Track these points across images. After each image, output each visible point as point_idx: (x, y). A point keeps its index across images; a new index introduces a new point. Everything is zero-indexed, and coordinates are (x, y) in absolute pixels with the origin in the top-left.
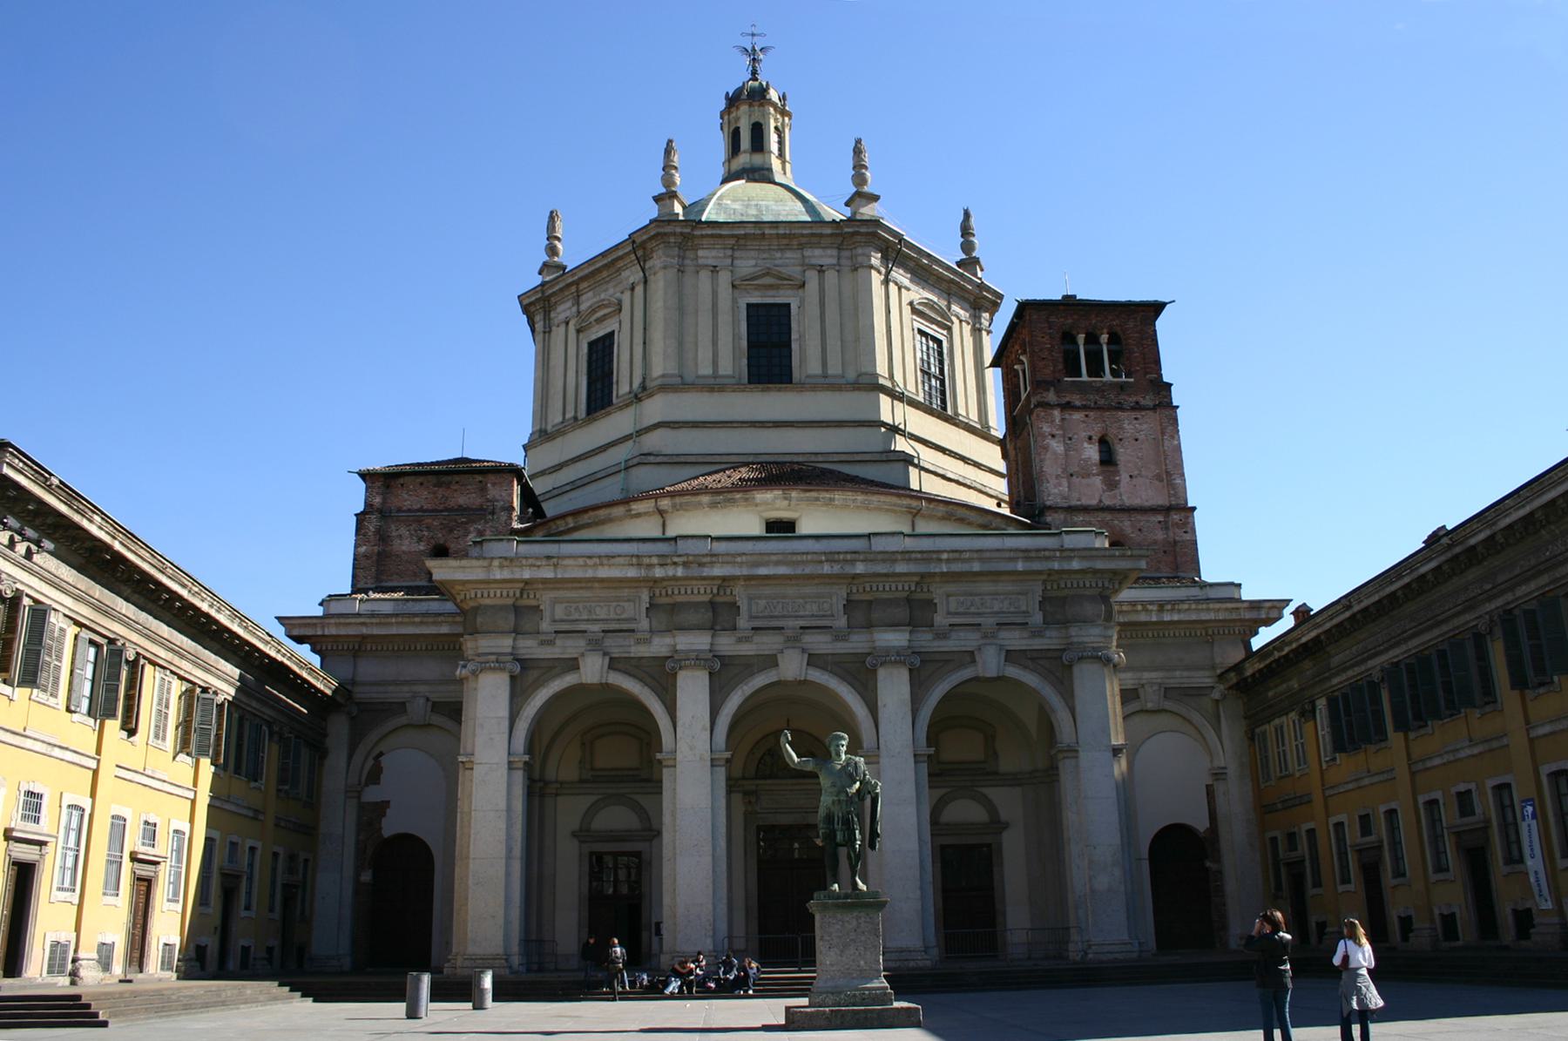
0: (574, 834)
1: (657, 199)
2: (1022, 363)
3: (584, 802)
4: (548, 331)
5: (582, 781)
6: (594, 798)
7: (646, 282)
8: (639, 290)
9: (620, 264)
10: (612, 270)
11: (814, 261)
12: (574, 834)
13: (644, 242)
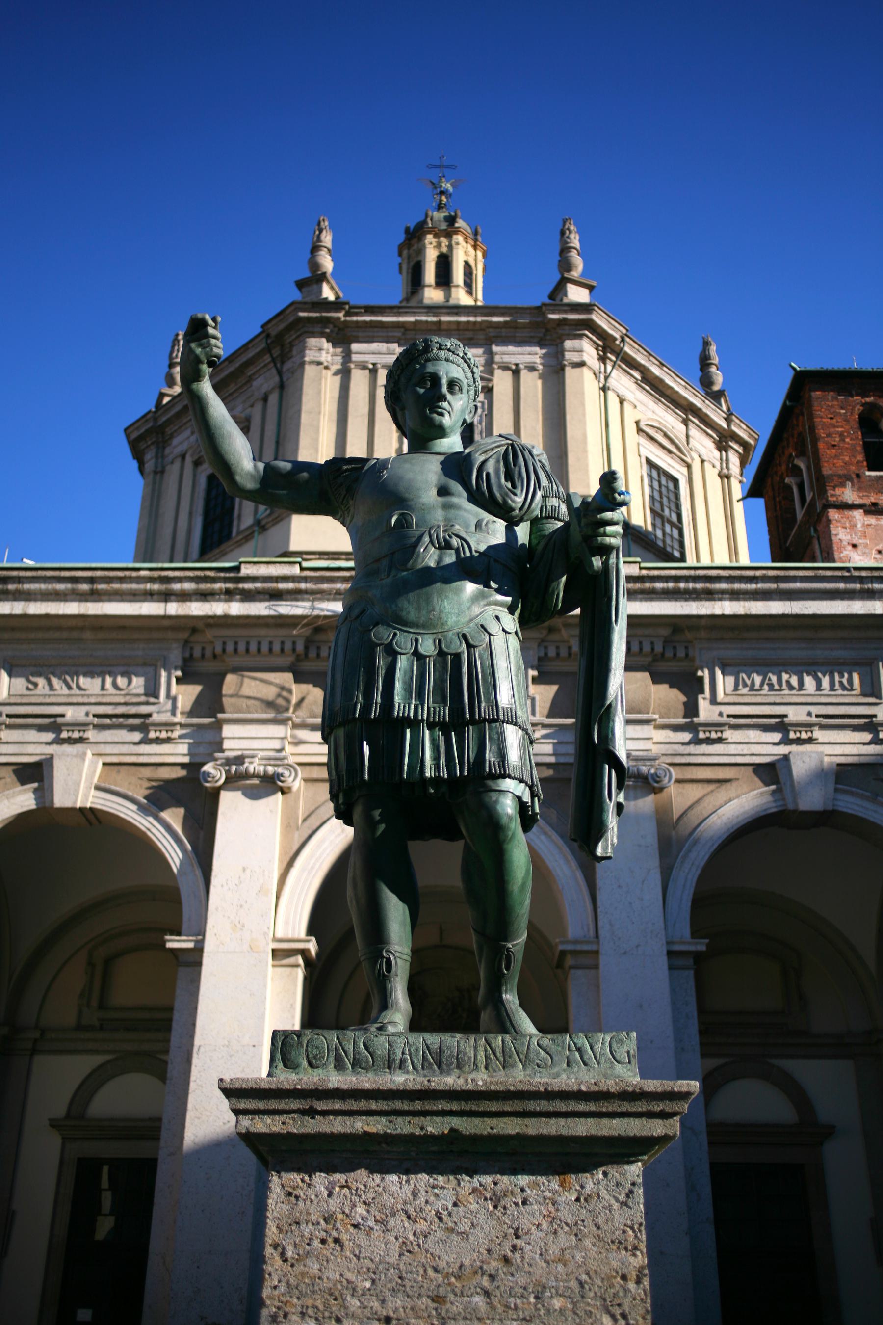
0: (54, 1124)
1: (301, 284)
2: (796, 471)
3: (81, 1065)
4: (160, 472)
5: (79, 1027)
6: (97, 1060)
7: (282, 386)
8: (273, 399)
9: (250, 371)
10: (242, 380)
11: (506, 359)
12: (54, 1124)
13: (280, 336)
